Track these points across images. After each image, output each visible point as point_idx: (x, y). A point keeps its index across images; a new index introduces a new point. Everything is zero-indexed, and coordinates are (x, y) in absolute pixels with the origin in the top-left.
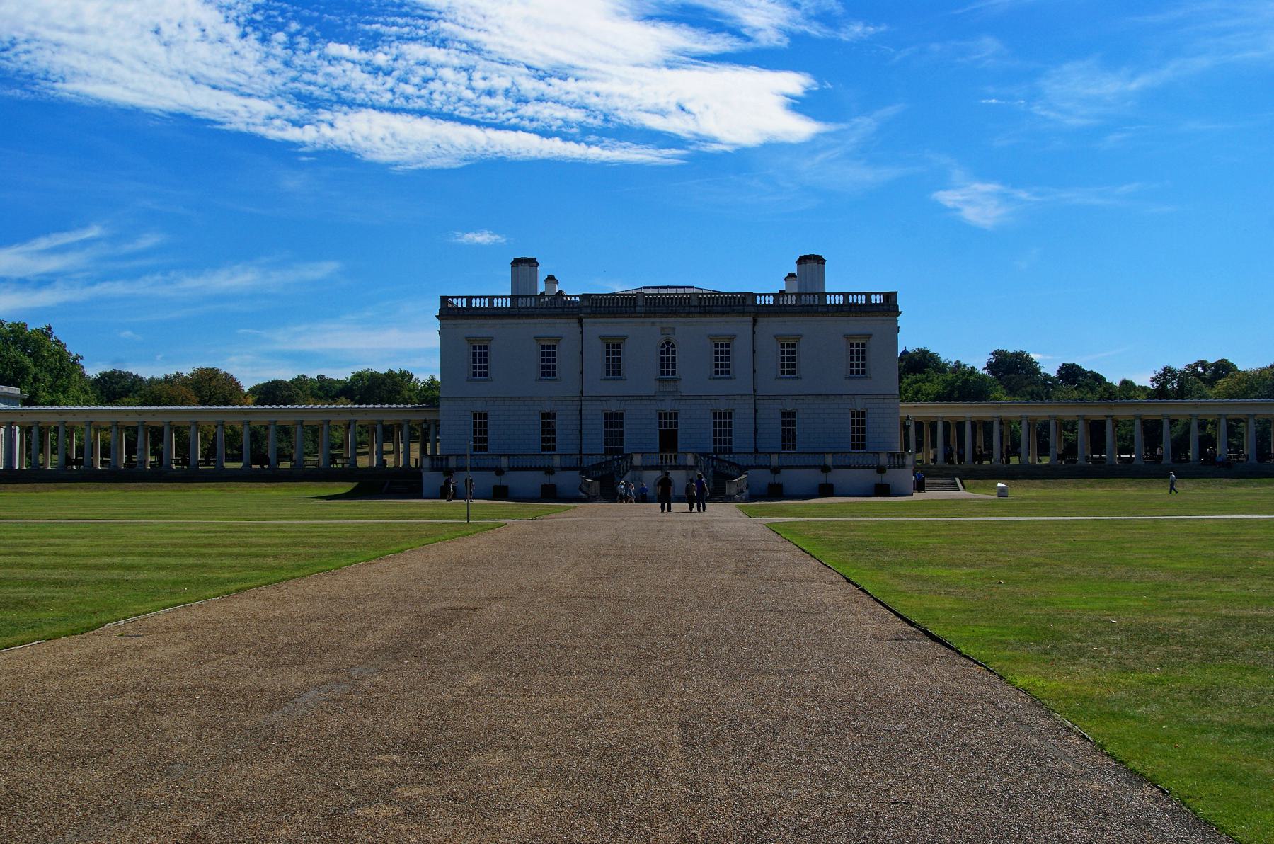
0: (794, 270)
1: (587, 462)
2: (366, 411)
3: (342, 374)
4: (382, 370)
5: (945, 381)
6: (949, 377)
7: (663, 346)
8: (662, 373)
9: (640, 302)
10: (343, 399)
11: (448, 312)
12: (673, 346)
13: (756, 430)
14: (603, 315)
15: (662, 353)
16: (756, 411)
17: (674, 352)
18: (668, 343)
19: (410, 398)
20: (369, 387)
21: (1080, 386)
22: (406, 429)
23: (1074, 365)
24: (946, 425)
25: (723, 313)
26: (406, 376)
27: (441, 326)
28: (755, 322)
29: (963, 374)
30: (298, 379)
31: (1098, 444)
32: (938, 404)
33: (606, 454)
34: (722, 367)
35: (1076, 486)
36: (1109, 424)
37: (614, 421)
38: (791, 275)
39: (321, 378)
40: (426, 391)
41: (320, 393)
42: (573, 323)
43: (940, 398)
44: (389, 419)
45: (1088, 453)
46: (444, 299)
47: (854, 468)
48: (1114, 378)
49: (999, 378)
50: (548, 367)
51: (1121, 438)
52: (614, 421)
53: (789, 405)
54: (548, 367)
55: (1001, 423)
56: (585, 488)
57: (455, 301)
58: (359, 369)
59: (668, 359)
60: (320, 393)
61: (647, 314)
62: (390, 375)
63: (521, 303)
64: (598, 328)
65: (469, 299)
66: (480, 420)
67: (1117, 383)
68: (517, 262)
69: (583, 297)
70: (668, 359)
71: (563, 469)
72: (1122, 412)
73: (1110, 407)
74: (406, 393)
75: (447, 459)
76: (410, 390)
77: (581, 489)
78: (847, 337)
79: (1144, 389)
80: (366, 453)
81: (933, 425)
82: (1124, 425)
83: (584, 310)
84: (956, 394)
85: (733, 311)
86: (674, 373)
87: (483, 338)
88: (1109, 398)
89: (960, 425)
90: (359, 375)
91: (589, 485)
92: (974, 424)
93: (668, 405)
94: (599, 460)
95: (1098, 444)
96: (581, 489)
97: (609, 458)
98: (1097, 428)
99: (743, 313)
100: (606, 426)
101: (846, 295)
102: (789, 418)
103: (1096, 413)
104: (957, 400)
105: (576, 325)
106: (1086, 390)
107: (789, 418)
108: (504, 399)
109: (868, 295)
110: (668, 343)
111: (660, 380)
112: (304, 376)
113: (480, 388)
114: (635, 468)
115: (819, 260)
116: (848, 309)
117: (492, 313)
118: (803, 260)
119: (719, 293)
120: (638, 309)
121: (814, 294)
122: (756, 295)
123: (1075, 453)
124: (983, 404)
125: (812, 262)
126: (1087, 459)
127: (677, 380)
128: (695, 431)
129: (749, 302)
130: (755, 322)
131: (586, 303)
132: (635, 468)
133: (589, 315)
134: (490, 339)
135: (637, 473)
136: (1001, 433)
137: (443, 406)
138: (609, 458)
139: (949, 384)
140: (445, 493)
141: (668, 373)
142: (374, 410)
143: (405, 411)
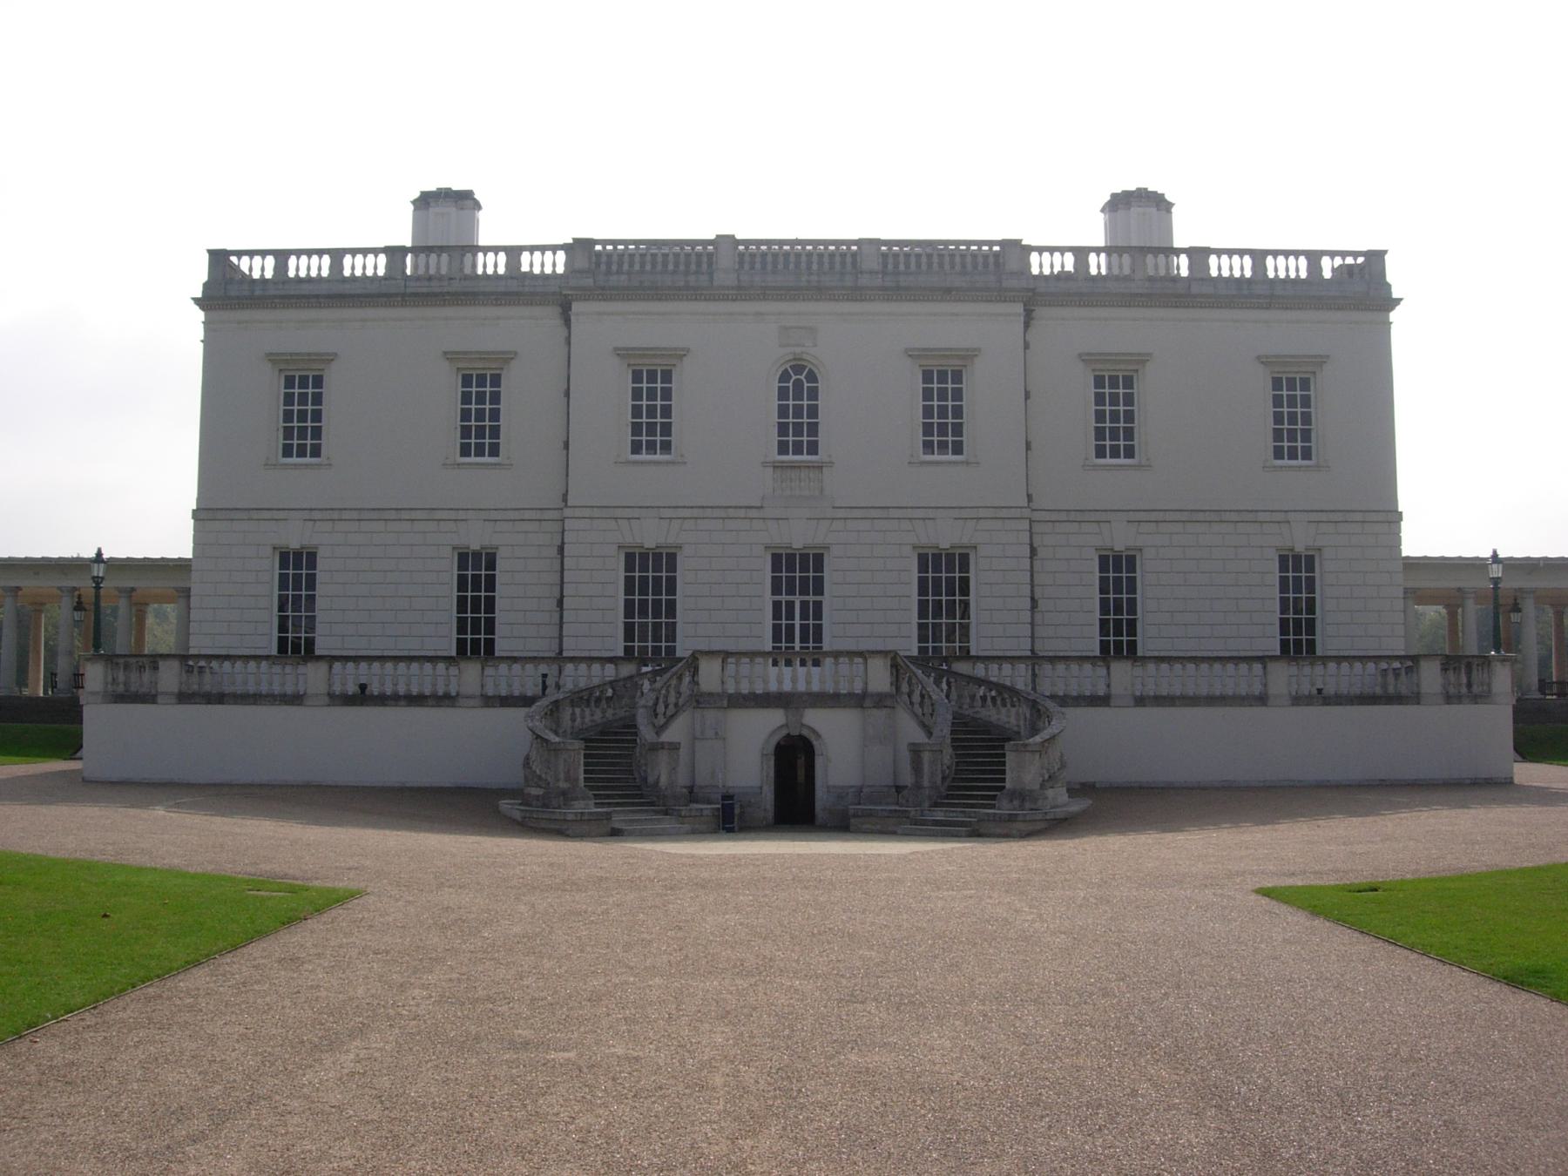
7: (785, 377)
8: (783, 448)
9: (725, 261)
12: (812, 377)
15: (783, 393)
17: (813, 394)
18: (798, 369)
34: (943, 427)
37: (651, 579)
46: (219, 259)
50: (480, 432)
52: (651, 579)
53: (1121, 539)
54: (480, 432)
57: (244, 264)
59: (798, 412)
61: (741, 292)
65: (282, 256)
66: (297, 568)
69: (579, 248)
70: (798, 412)
86: (813, 448)
93: (798, 536)
99: (1000, 294)
101: (1259, 256)
102: (1118, 572)
105: (559, 322)
107: (1118, 572)
109: (1314, 257)
110: (798, 369)
111: (776, 466)
113: (301, 483)
116: (1258, 294)
122: (1029, 249)
127: (819, 467)
128: (872, 606)
129: (1012, 265)
131: (582, 263)
133: (588, 294)
135: (711, 715)
141: (798, 449)
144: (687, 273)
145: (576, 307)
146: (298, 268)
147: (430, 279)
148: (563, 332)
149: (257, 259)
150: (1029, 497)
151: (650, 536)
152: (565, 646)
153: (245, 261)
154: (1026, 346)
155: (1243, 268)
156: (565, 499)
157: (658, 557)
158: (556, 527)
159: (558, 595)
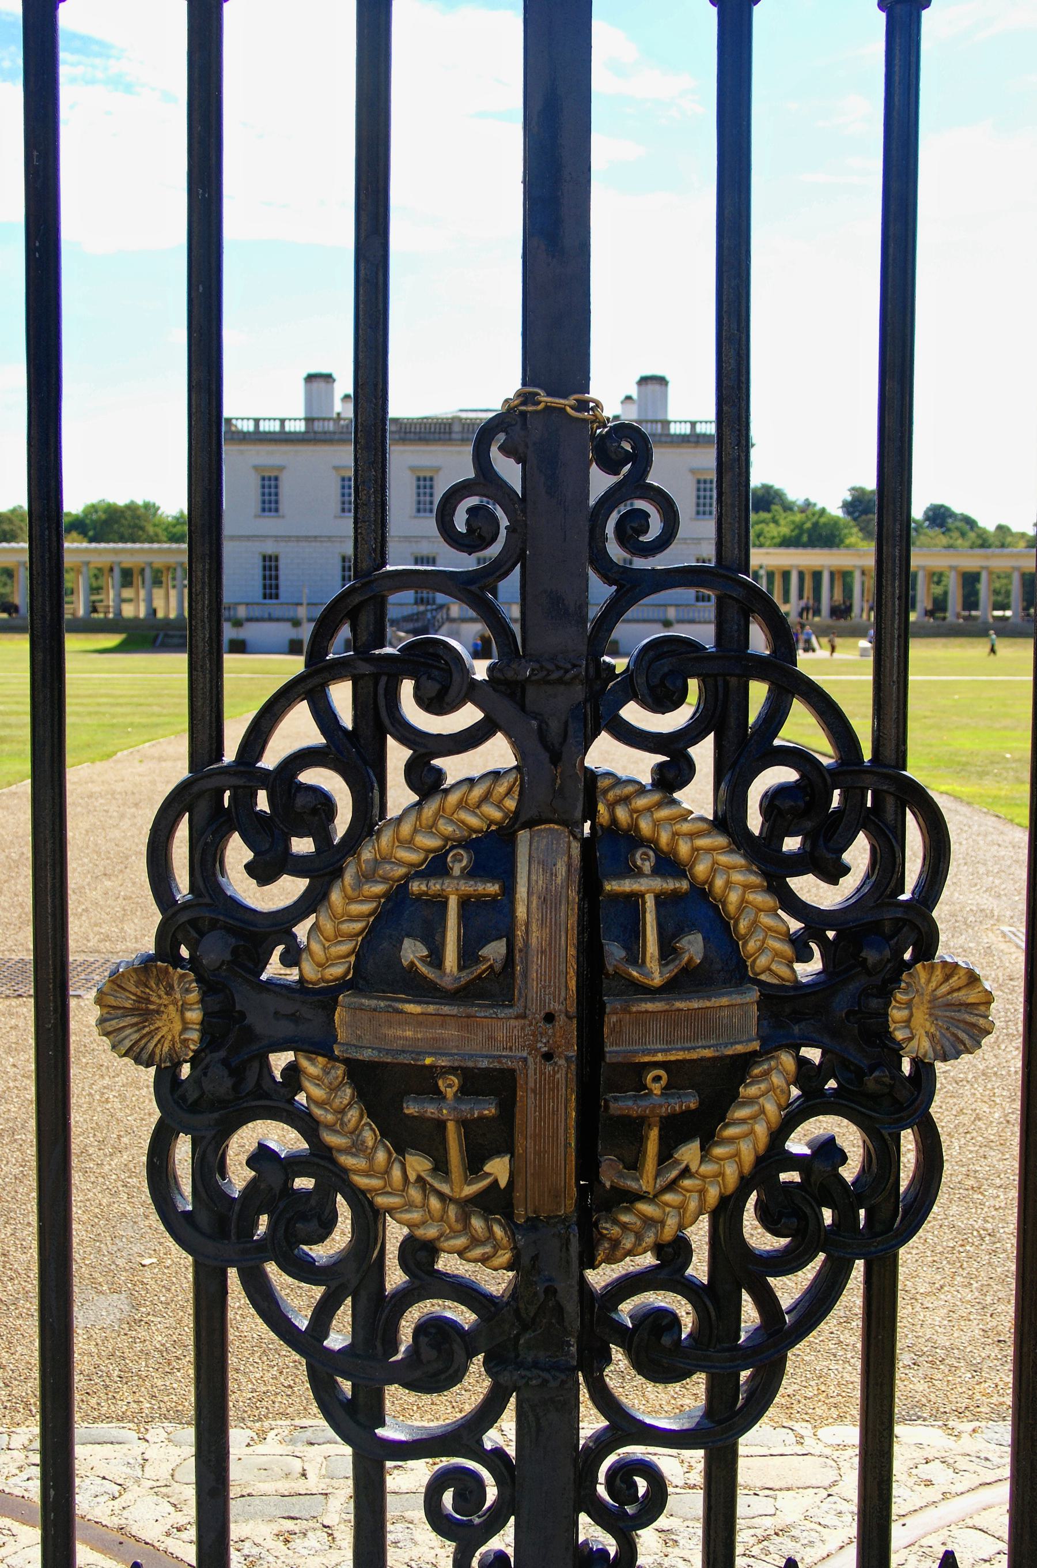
0: (634, 392)
2: (132, 552)
4: (121, 501)
5: (793, 522)
6: (798, 517)
9: (457, 428)
14: (412, 442)
19: (157, 535)
21: (949, 530)
22: (148, 573)
23: (942, 506)
24: (801, 575)
26: (150, 508)
29: (814, 514)
31: (971, 601)
32: (782, 551)
33: (416, 603)
35: (945, 646)
36: (984, 577)
38: (628, 398)
40: (174, 526)
43: (787, 543)
44: (128, 562)
45: (959, 608)
47: (699, 622)
48: (988, 523)
49: (855, 519)
51: (996, 592)
55: (863, 573)
62: (131, 507)
63: (318, 426)
66: (270, 565)
67: (991, 528)
68: (311, 378)
72: (999, 562)
73: (987, 557)
74: (151, 530)
76: (155, 525)
78: (693, 471)
79: (1023, 535)
80: (130, 600)
81: (786, 575)
82: (999, 577)
84: (805, 538)
87: (273, 468)
88: (982, 546)
89: (817, 576)
90: (93, 506)
92: (832, 574)
95: (971, 601)
98: (970, 580)
103: (971, 562)
104: (804, 546)
106: (956, 534)
108: (299, 539)
115: (662, 381)
117: (283, 438)
118: (644, 381)
120: (454, 436)
121: (657, 422)
123: (944, 609)
124: (835, 551)
125: (654, 382)
126: (958, 616)
134: (282, 468)
136: (863, 584)
138: (422, 608)
139: (799, 527)
146: (264, 426)
147: (325, 433)
149: (245, 421)
153: (240, 421)
155: (686, 429)
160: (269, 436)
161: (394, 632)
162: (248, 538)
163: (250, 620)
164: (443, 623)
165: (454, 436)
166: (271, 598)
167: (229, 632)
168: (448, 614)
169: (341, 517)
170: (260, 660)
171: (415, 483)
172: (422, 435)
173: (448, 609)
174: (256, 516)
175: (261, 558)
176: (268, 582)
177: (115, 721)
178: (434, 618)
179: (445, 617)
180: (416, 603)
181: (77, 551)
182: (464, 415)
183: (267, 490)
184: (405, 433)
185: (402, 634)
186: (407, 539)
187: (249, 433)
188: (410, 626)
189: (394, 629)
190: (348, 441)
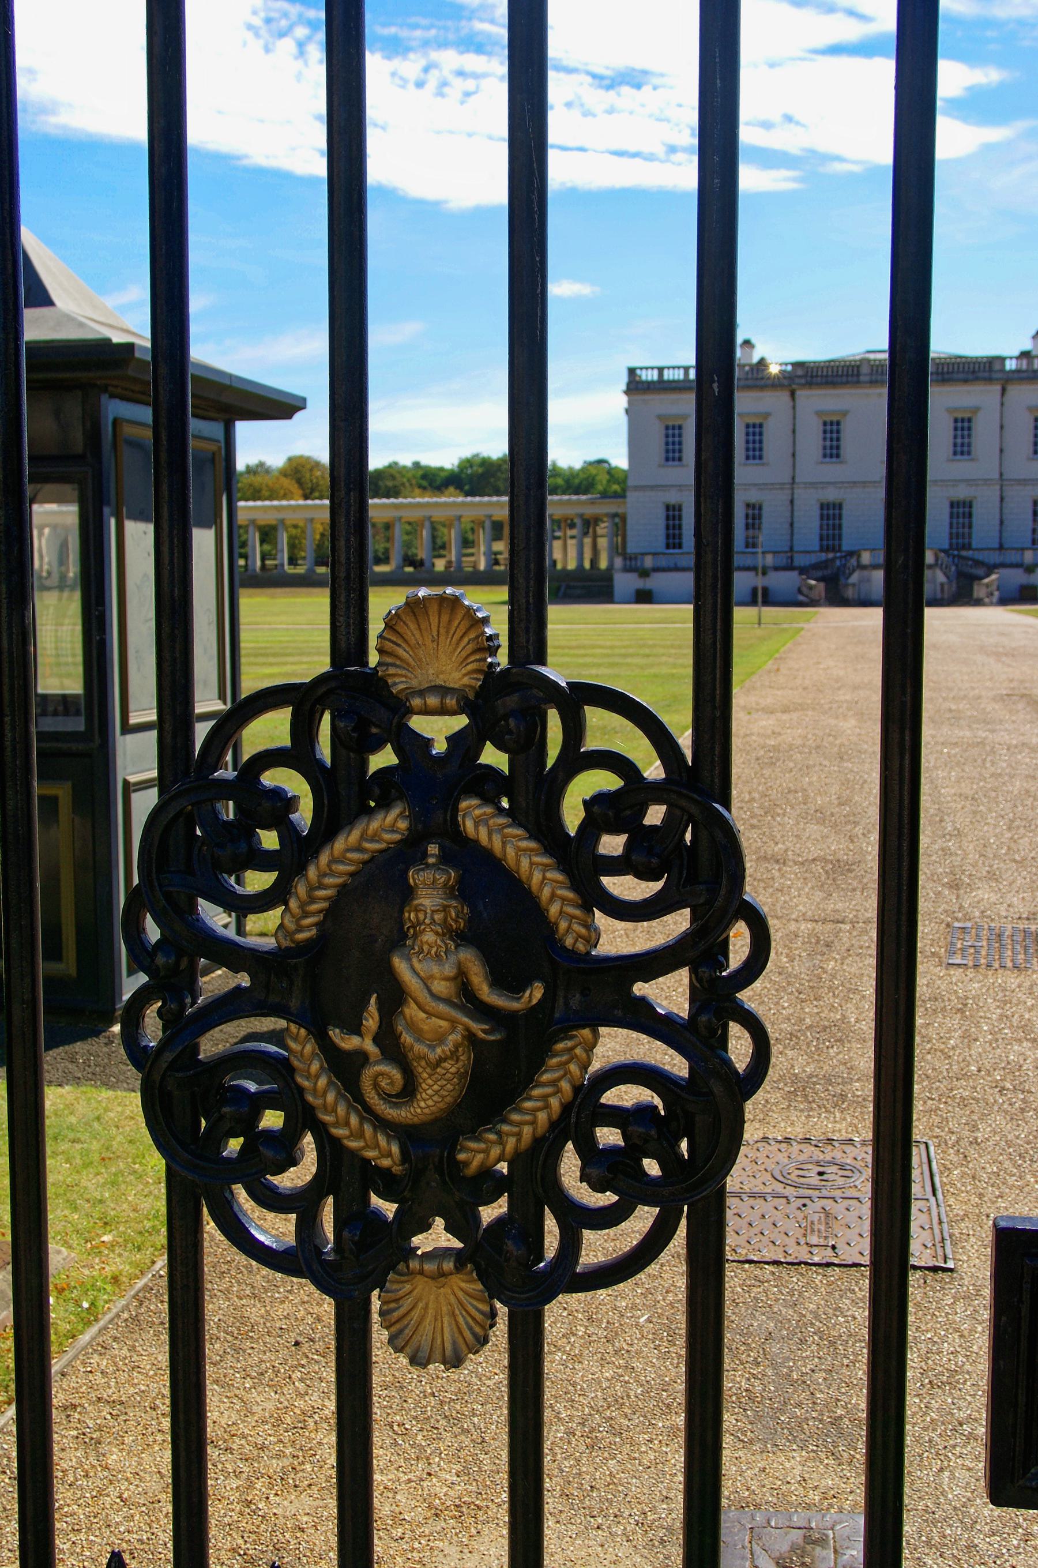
1: (800, 560)
3: (446, 459)
9: (865, 370)
10: (451, 489)
11: (635, 386)
13: (1002, 522)
16: (1002, 499)
20: (482, 475)
25: (966, 381)
27: (629, 402)
28: (1004, 391)
30: (390, 466)
33: (821, 550)
37: (831, 514)
39: (417, 465)
41: (424, 483)
42: (784, 396)
46: (632, 371)
52: (831, 514)
56: (805, 590)
58: (467, 453)
60: (424, 483)
64: (815, 402)
71: (776, 569)
75: (643, 560)
77: (800, 591)
83: (797, 381)
85: (977, 379)
91: (811, 588)
94: (813, 559)
96: (800, 591)
97: (831, 555)
99: (990, 380)
100: (822, 519)
112: (396, 463)
114: (864, 567)
119: (960, 357)
120: (862, 378)
129: (997, 366)
130: (1004, 391)
131: (800, 372)
132: (864, 567)
133: (803, 386)
135: (866, 573)
137: (631, 496)
138: (831, 555)
140: (644, 597)
142: (480, 504)
143: (579, 502)
144: (847, 375)
145: (798, 393)
146: (668, 375)
148: (791, 404)
150: (1001, 474)
151: (831, 495)
152: (795, 543)
154: (1002, 404)
156: (793, 478)
157: (834, 505)
158: (790, 492)
159: (789, 520)
160: (674, 385)
161: (804, 580)
162: (652, 488)
163: (656, 570)
164: (854, 571)
165: (995, 376)
166: (674, 548)
167: (742, 582)
168: (858, 561)
169: (953, 460)
170: (679, 610)
171: (952, 425)
172: (946, 376)
173: (859, 556)
174: (949, 460)
175: (818, 506)
176: (677, 532)
177: (674, 671)
178: (845, 565)
179: (855, 564)
180: (821, 550)
181: (561, 503)
182: (872, 356)
183: (751, 438)
184: (812, 377)
185: (813, 582)
186: (813, 485)
187: (652, 382)
188: (820, 574)
189: (804, 577)
190: (882, 382)
